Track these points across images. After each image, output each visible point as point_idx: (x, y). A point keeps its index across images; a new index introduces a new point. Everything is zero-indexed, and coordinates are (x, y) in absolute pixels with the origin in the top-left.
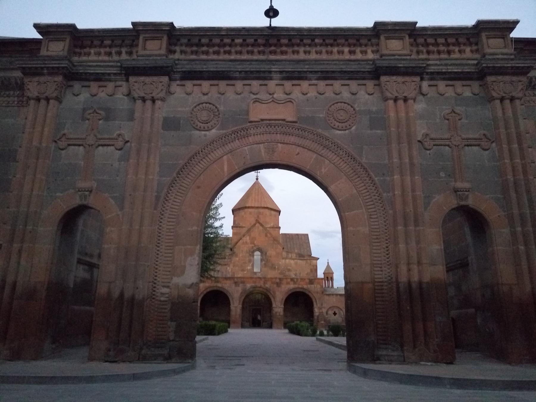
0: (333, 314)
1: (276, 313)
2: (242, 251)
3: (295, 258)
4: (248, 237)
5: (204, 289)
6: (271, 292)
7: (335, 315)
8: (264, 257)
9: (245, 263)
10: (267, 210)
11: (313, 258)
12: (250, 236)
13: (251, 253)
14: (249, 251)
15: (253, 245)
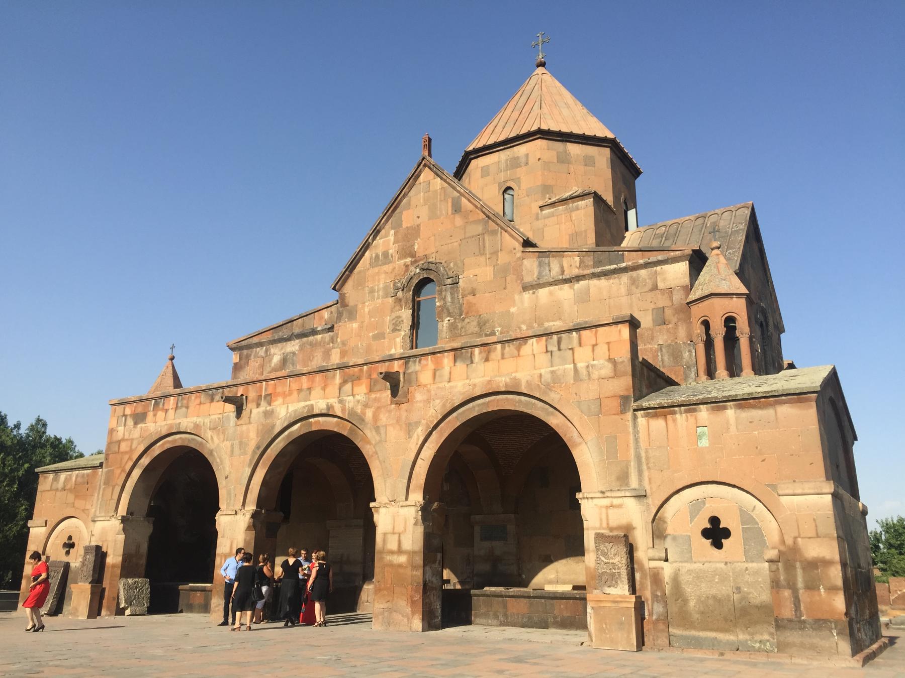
0: (706, 533)
1: (385, 534)
2: (372, 291)
3: (576, 272)
4: (392, 232)
5: (141, 448)
6: (370, 433)
7: (718, 545)
8: (449, 299)
9: (380, 336)
10: (540, 143)
11: (660, 257)
12: (397, 226)
13: (400, 294)
14: (394, 285)
15: (408, 260)
